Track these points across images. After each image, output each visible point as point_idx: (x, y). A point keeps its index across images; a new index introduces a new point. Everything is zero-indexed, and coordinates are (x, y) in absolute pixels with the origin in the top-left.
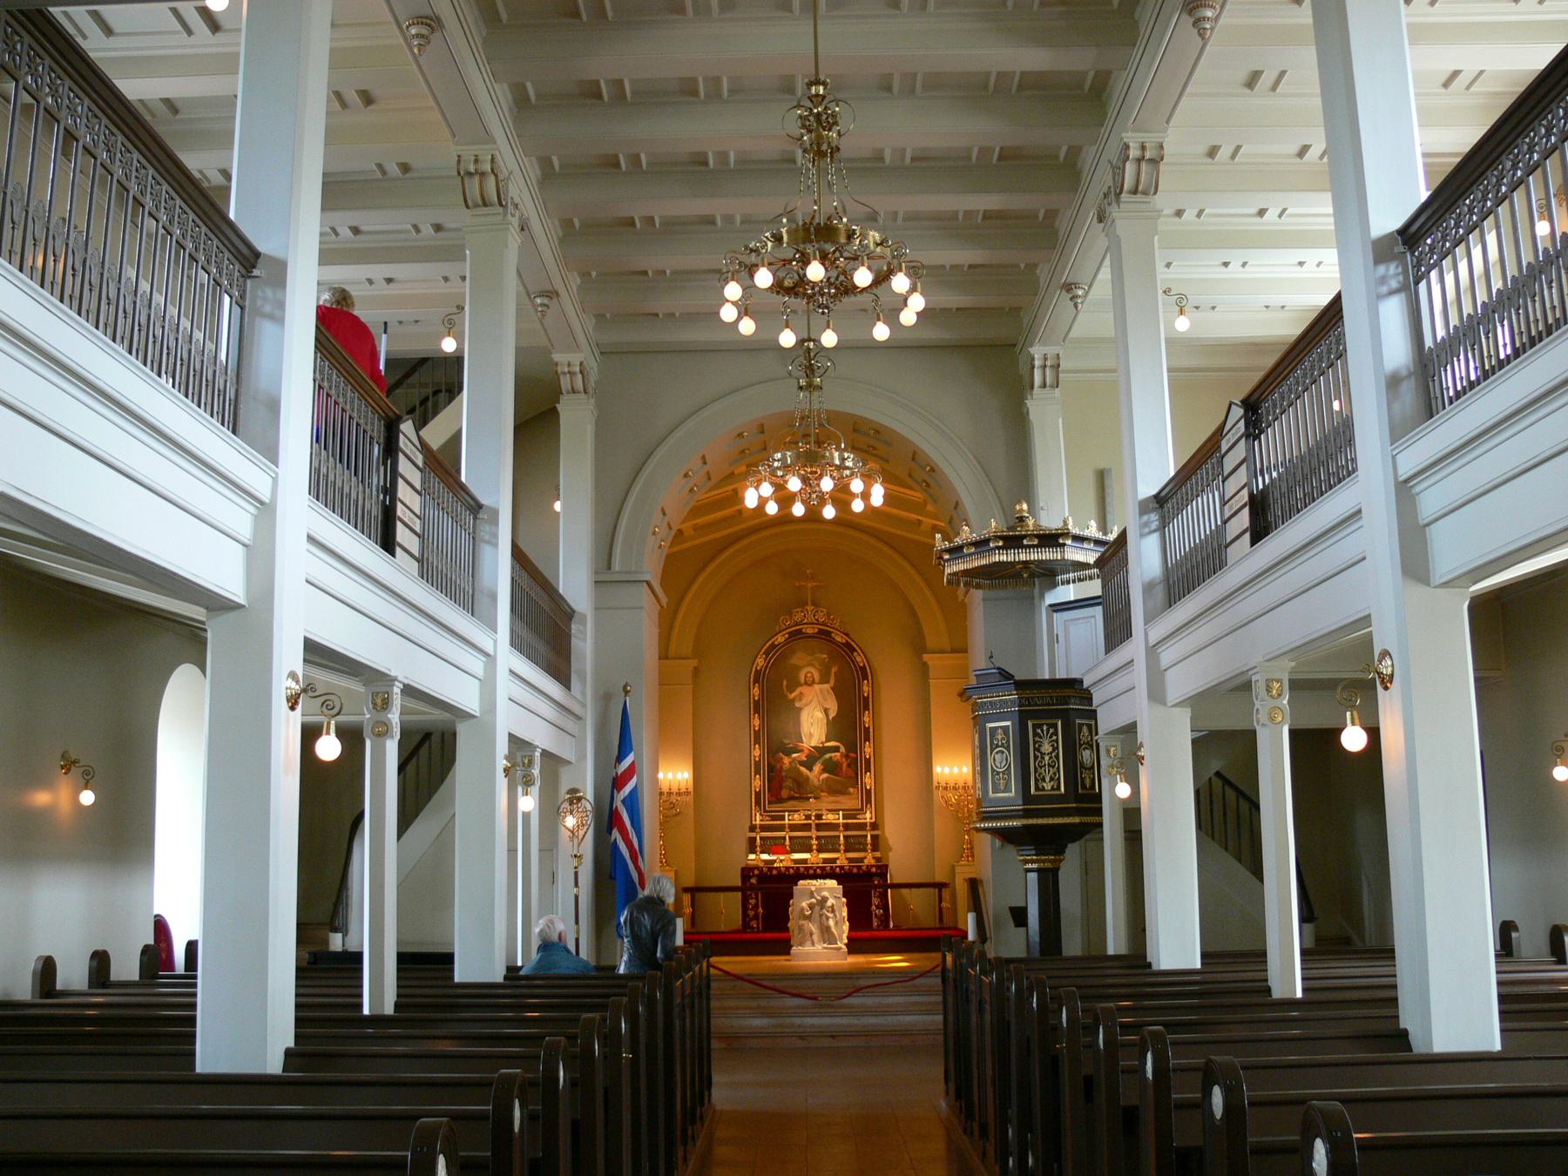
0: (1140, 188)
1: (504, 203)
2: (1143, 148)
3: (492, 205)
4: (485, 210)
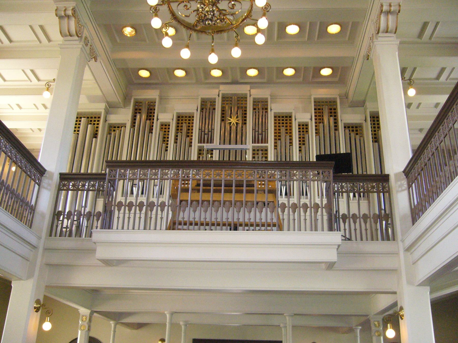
0: (389, 30)
1: (80, 36)
2: (390, 6)
3: (73, 36)
4: (69, 38)
